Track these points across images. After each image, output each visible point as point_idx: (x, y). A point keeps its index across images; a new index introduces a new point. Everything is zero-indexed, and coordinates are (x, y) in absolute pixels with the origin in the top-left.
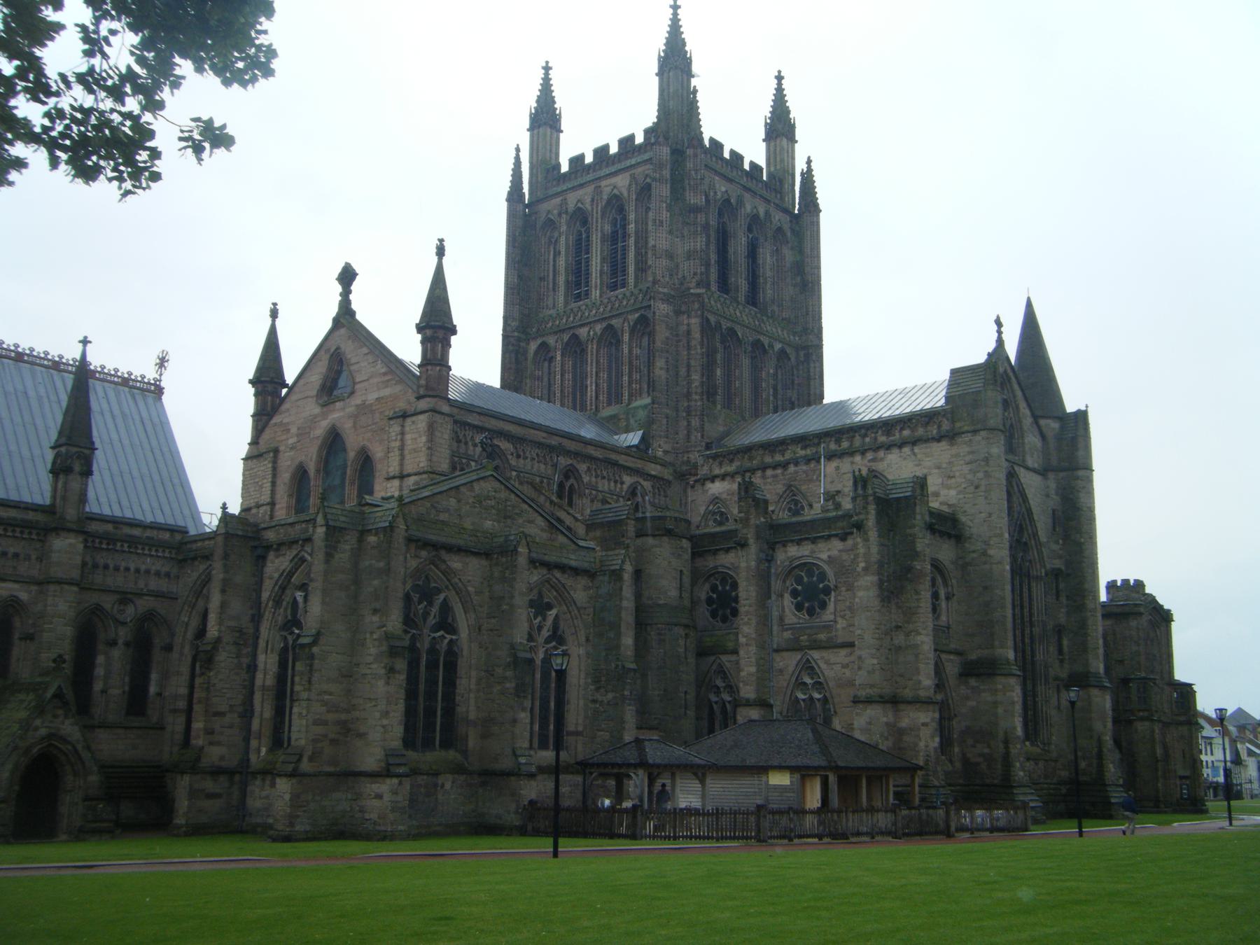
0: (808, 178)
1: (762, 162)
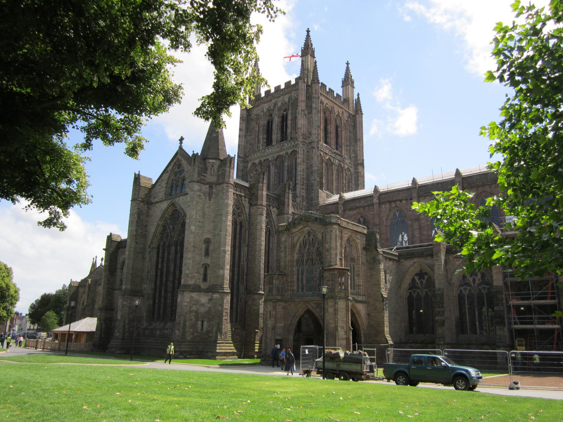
0: (358, 101)
1: (341, 94)
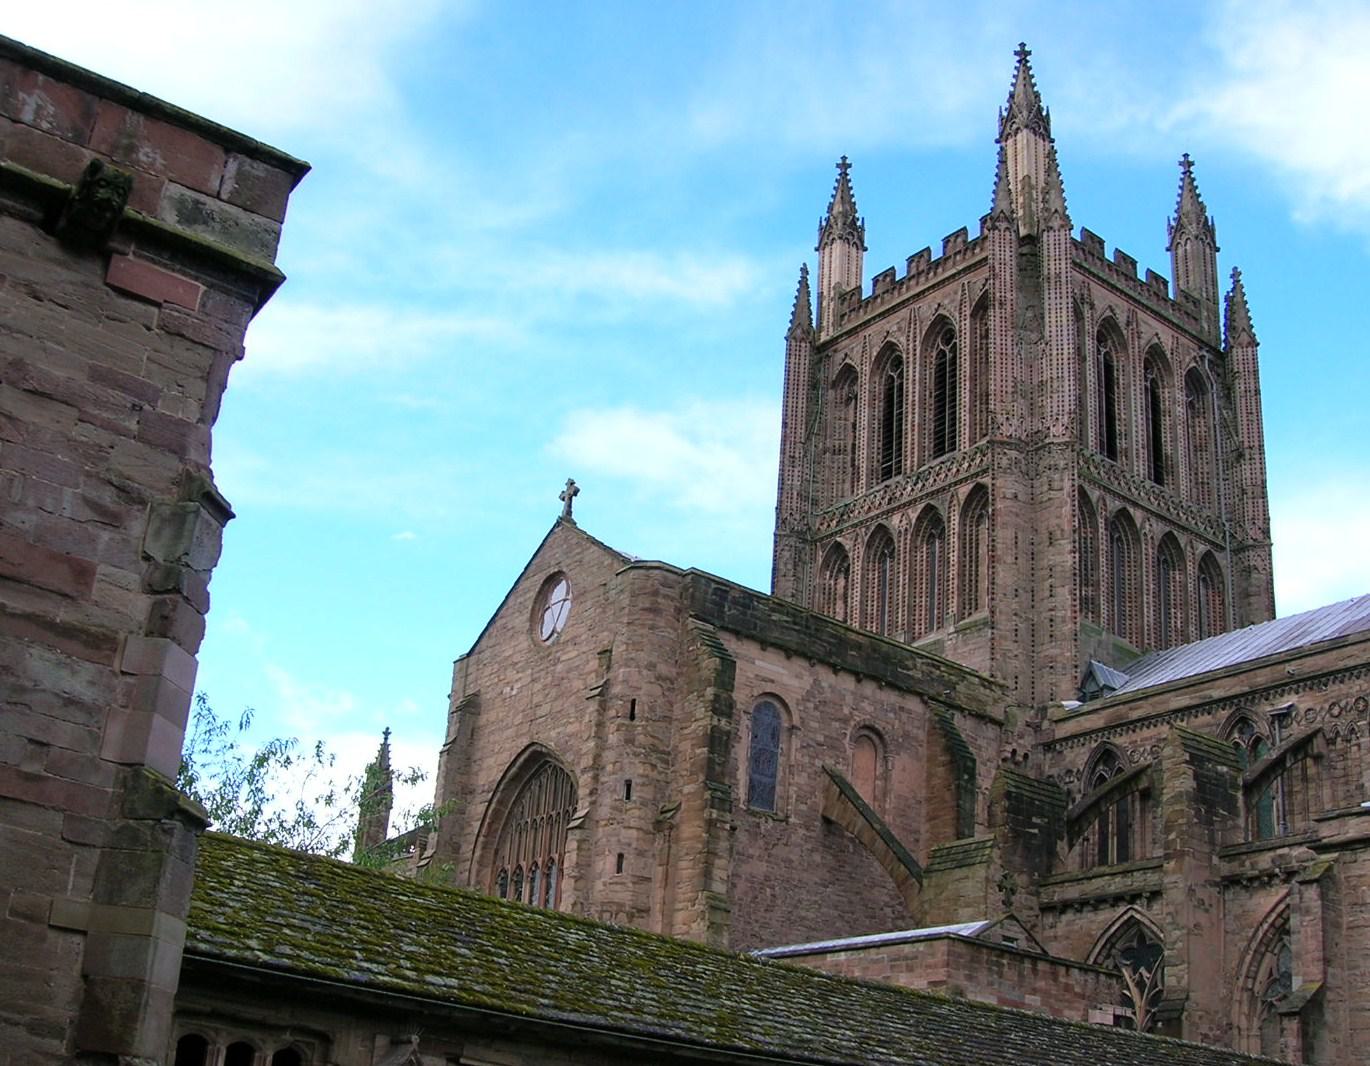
1: (1165, 270)
